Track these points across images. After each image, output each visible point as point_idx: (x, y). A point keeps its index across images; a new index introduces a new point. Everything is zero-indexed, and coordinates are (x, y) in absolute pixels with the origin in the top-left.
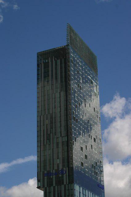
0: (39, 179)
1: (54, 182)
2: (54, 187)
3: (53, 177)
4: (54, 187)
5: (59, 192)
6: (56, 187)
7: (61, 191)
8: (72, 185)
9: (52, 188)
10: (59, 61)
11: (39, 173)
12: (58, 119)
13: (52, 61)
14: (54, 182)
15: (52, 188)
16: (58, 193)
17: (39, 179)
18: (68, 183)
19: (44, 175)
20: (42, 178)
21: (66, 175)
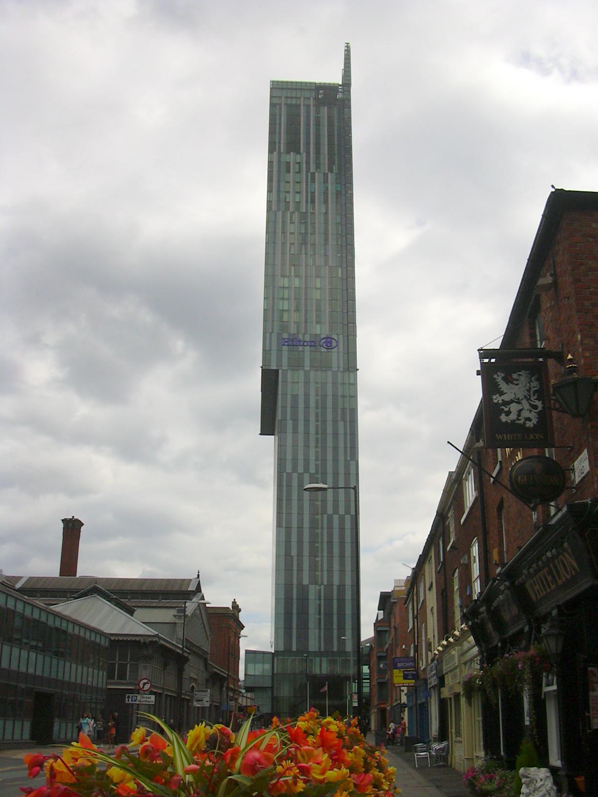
0: (268, 349)
1: (307, 362)
2: (307, 374)
3: (303, 351)
4: (307, 374)
5: (319, 386)
6: (312, 373)
7: (324, 384)
8: (352, 375)
9: (302, 373)
10: (325, 110)
11: (268, 334)
12: (319, 227)
13: (308, 106)
14: (307, 362)
15: (302, 373)
16: (317, 388)
17: (268, 349)
18: (342, 369)
19: (282, 342)
20: (274, 347)
21: (338, 352)
